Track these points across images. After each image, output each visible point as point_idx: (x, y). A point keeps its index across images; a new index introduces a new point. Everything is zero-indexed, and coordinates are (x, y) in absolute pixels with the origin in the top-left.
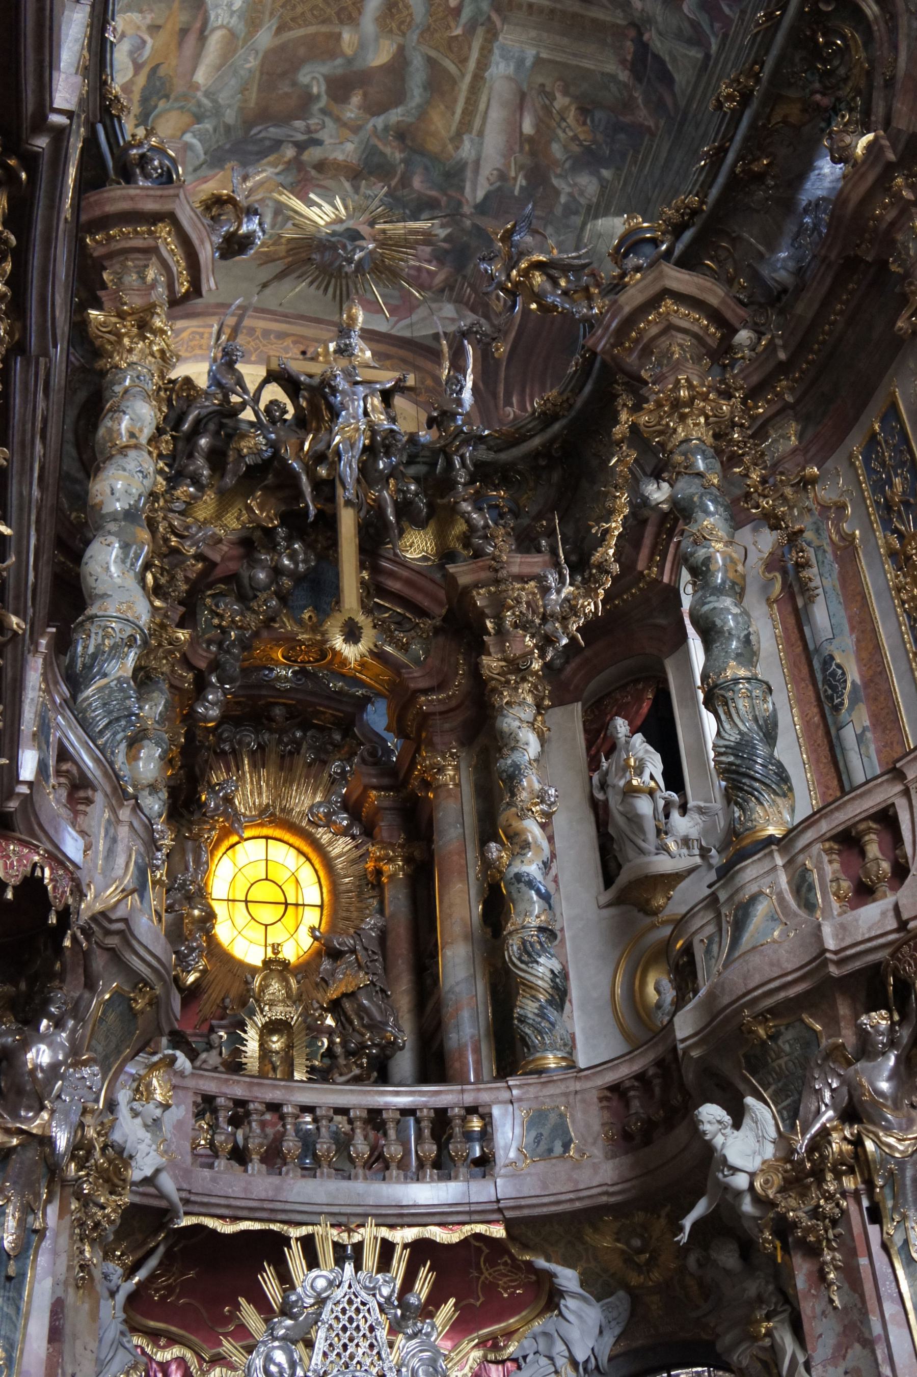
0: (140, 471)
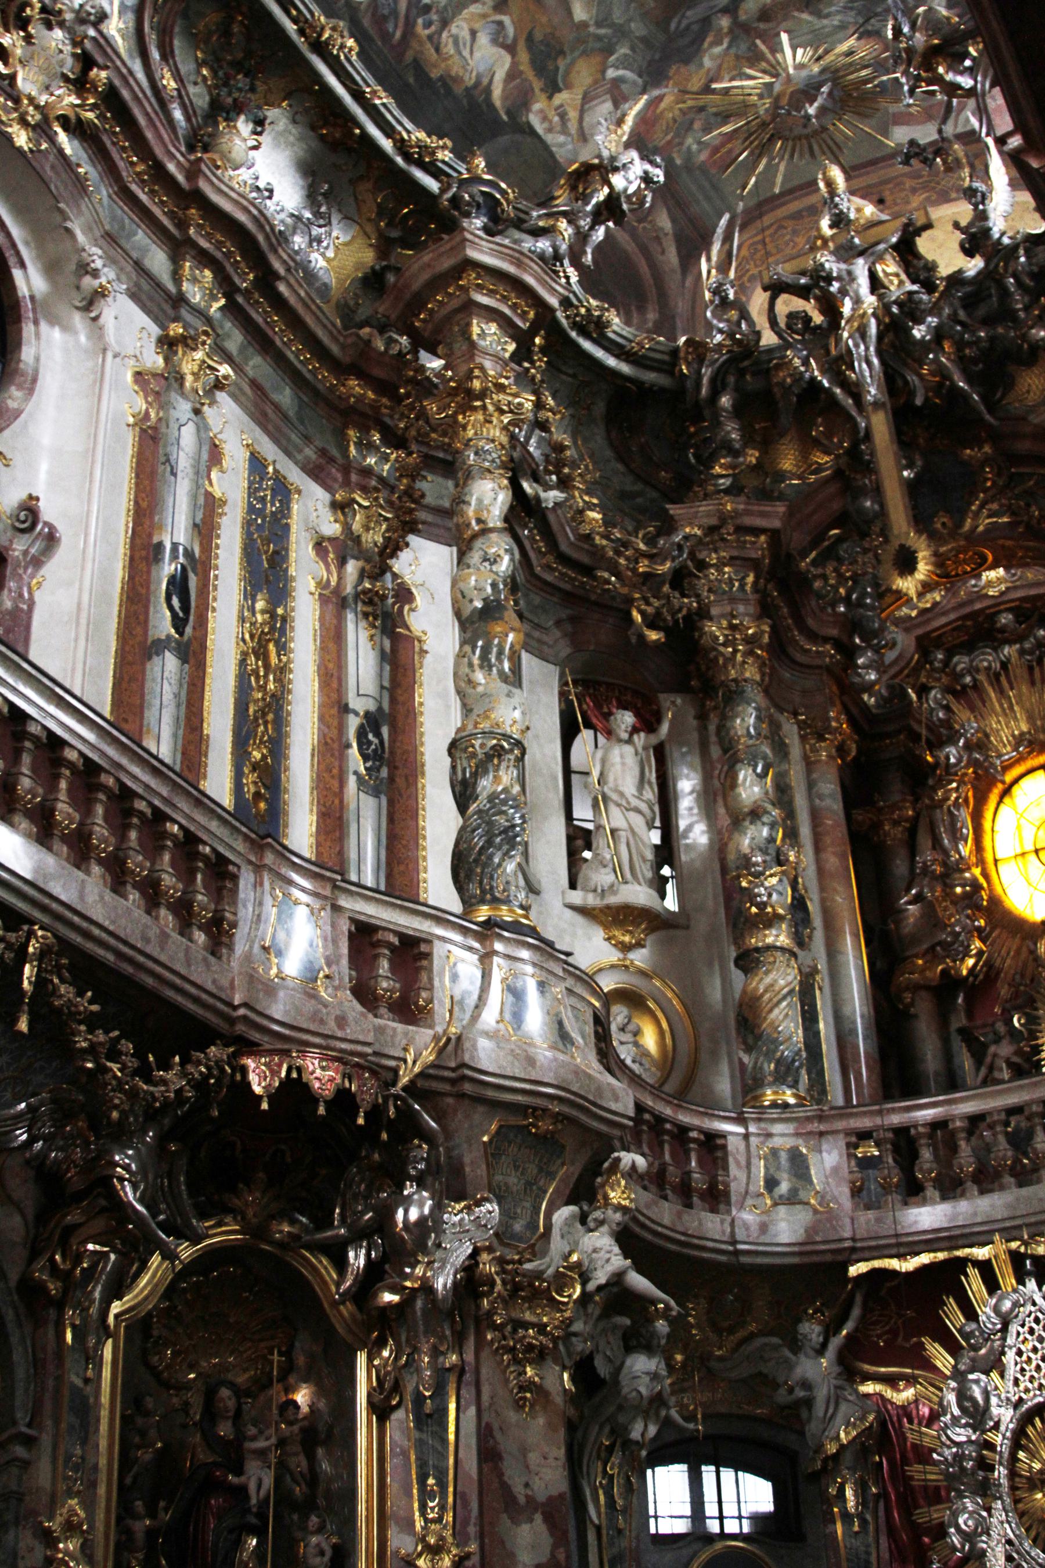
0: (485, 560)
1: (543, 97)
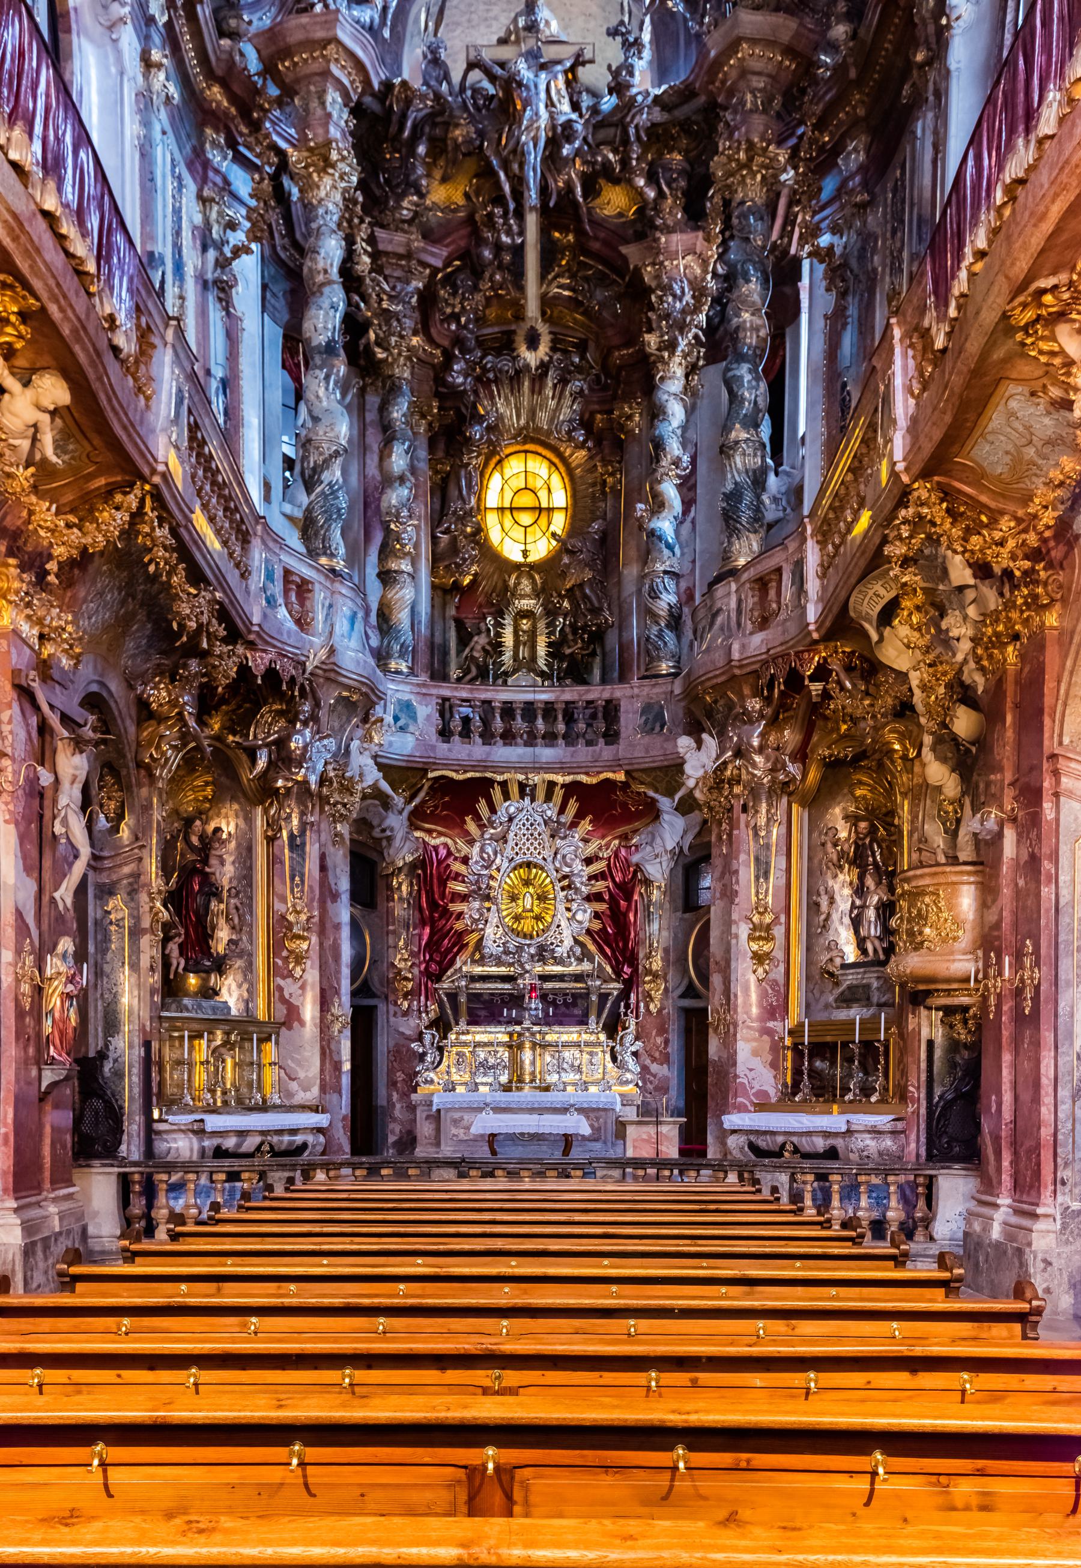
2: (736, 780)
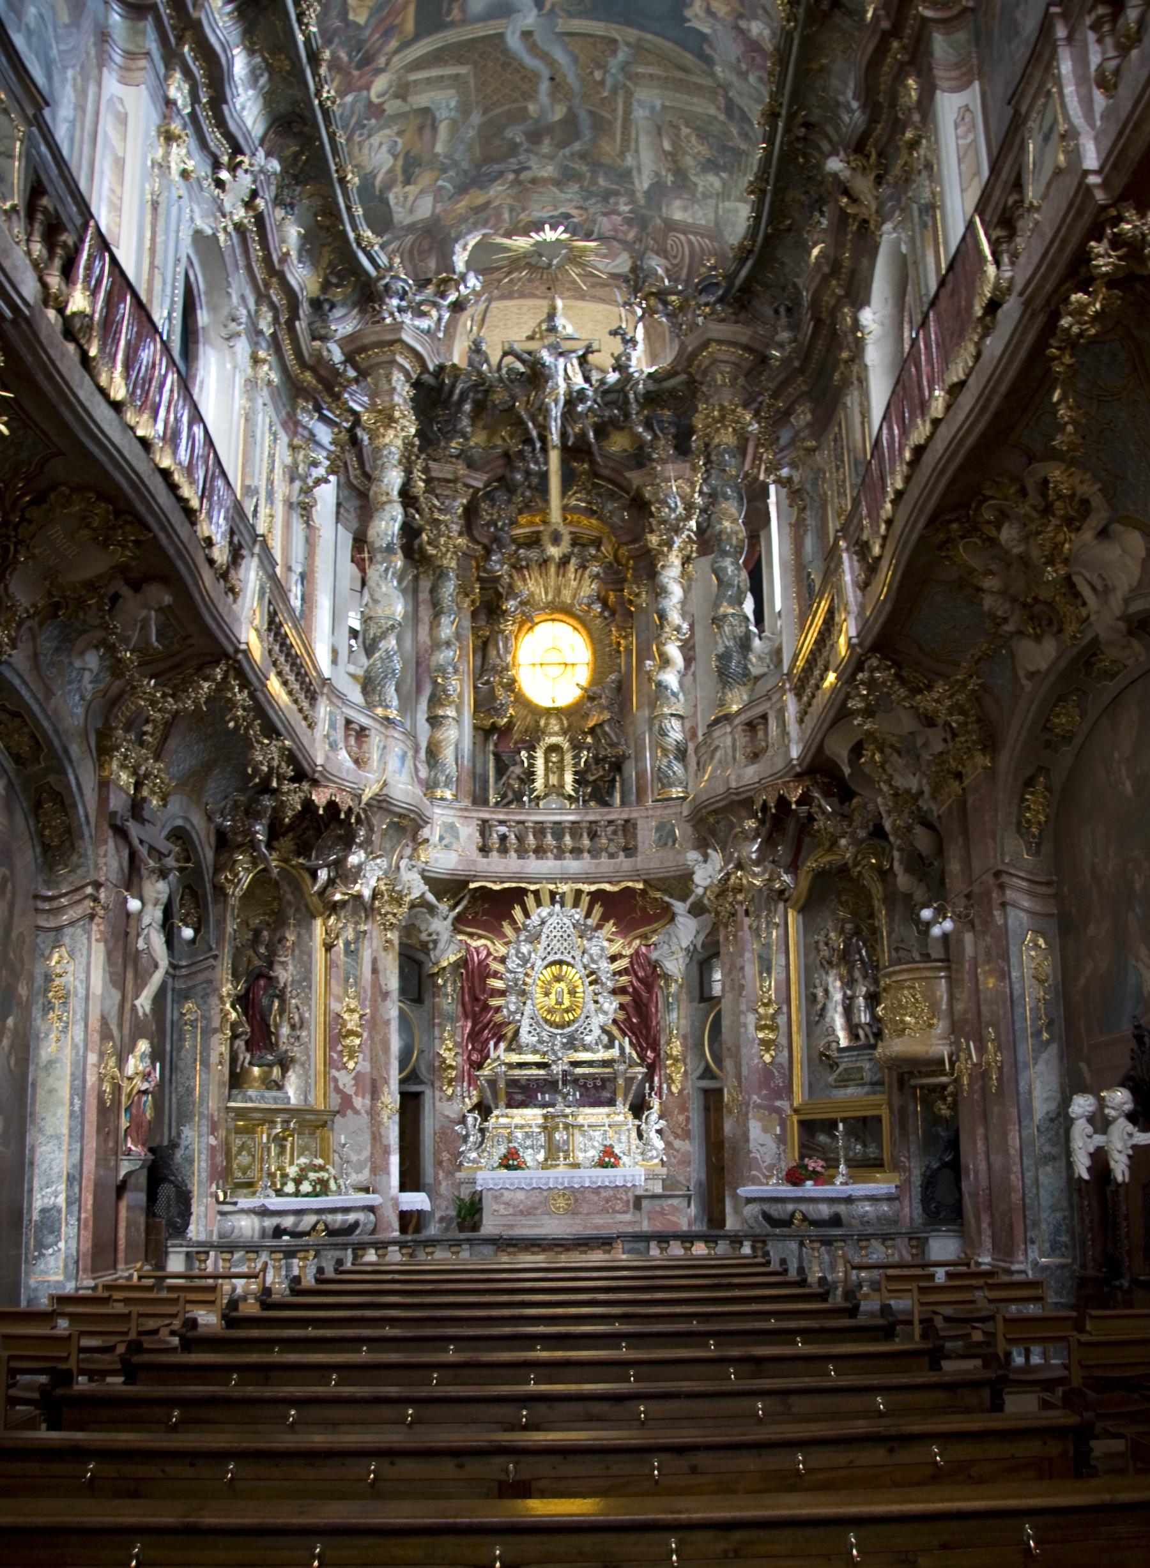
1: (399, 185)
2: (739, 889)
